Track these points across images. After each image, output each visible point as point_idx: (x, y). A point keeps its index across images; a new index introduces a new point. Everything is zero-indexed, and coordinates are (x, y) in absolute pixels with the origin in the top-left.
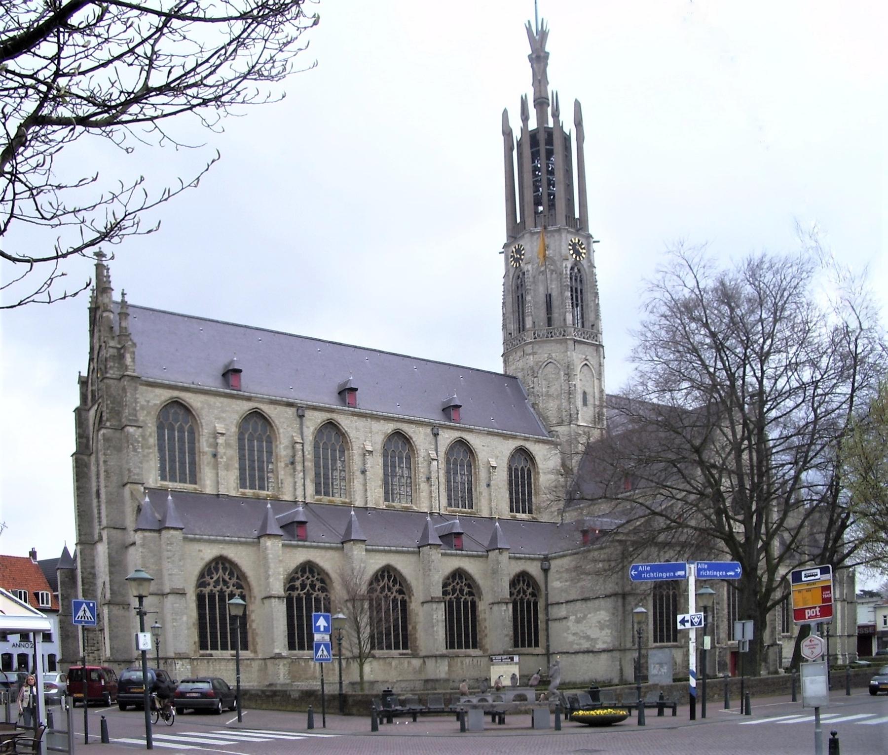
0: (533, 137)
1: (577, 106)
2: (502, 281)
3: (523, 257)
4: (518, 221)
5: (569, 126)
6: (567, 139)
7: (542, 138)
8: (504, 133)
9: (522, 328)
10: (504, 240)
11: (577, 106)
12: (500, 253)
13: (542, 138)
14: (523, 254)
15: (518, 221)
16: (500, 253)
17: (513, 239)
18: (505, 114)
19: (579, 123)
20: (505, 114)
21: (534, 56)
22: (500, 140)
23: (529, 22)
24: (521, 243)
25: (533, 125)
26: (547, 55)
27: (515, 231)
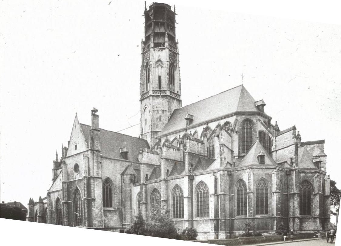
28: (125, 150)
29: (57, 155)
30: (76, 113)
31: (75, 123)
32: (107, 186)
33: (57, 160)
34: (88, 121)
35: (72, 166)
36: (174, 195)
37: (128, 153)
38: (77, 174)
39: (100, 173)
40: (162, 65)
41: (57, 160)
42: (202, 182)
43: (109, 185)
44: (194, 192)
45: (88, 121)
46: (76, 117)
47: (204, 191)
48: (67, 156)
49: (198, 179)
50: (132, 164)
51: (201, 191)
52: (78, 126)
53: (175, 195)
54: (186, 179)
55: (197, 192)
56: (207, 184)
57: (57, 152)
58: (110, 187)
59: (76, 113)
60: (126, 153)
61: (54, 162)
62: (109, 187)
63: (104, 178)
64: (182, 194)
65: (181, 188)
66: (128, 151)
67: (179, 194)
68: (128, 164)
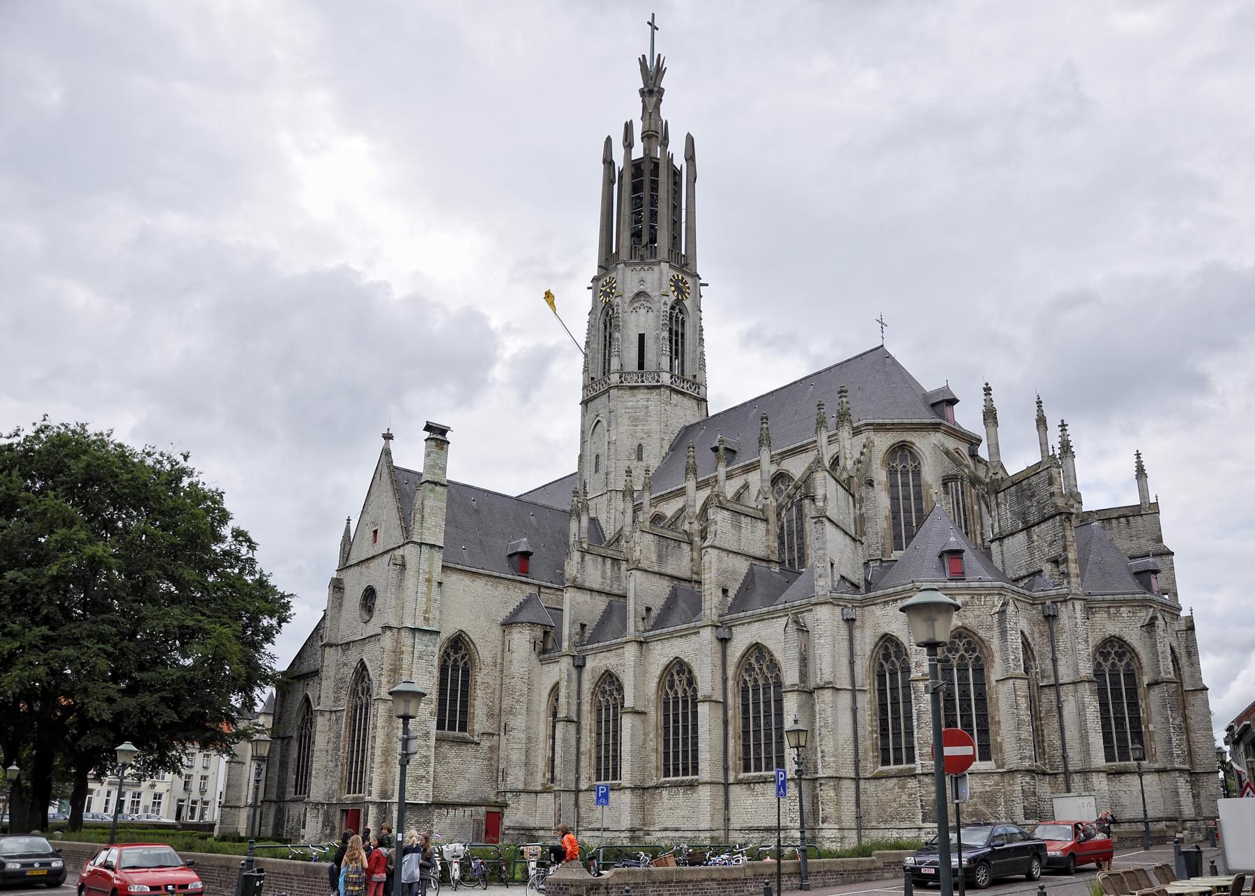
0: (637, 167)
1: (690, 141)
2: (588, 318)
3: (613, 291)
4: (614, 251)
5: (679, 162)
6: (676, 174)
7: (647, 168)
8: (604, 162)
9: (606, 371)
10: (594, 272)
11: (690, 141)
12: (588, 288)
13: (647, 168)
14: (615, 288)
15: (614, 251)
16: (588, 288)
17: (605, 271)
18: (609, 141)
19: (690, 157)
20: (609, 141)
21: (646, 90)
22: (600, 169)
23: (644, 56)
24: (613, 275)
25: (638, 152)
26: (661, 91)
27: (608, 261)
28: (522, 548)
31: (380, 467)
36: (667, 694)
37: (530, 557)
38: (368, 618)
39: (435, 613)
40: (648, 305)
42: (757, 649)
44: (730, 683)
47: (766, 678)
49: (742, 639)
50: (542, 590)
51: (756, 680)
53: (671, 695)
54: (707, 635)
55: (741, 684)
56: (778, 656)
60: (526, 555)
63: (448, 632)
64: (695, 690)
65: (690, 672)
66: (530, 550)
67: (685, 691)
68: (529, 590)
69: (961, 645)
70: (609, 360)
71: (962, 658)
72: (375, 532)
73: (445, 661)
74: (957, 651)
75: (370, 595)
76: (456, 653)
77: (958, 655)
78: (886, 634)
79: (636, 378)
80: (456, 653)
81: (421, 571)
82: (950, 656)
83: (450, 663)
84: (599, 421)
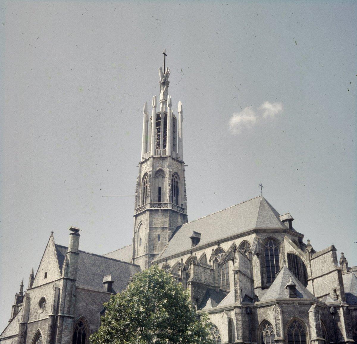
29: (22, 286)
30: (52, 232)
32: (80, 330)
33: (21, 293)
34: (67, 241)
35: (38, 300)
41: (21, 293)
43: (83, 328)
45: (67, 241)
46: (52, 236)
48: (33, 287)
52: (52, 248)
57: (22, 283)
58: (84, 331)
59: (52, 232)
61: (17, 295)
62: (82, 332)
63: (78, 318)
69: (295, 325)
70: (146, 198)
71: (296, 331)
72: (46, 274)
73: (75, 330)
74: (294, 328)
75: (42, 302)
76: (80, 326)
77: (294, 330)
78: (264, 320)
79: (157, 206)
80: (80, 326)
81: (67, 291)
82: (291, 330)
83: (78, 331)
84: (141, 224)
